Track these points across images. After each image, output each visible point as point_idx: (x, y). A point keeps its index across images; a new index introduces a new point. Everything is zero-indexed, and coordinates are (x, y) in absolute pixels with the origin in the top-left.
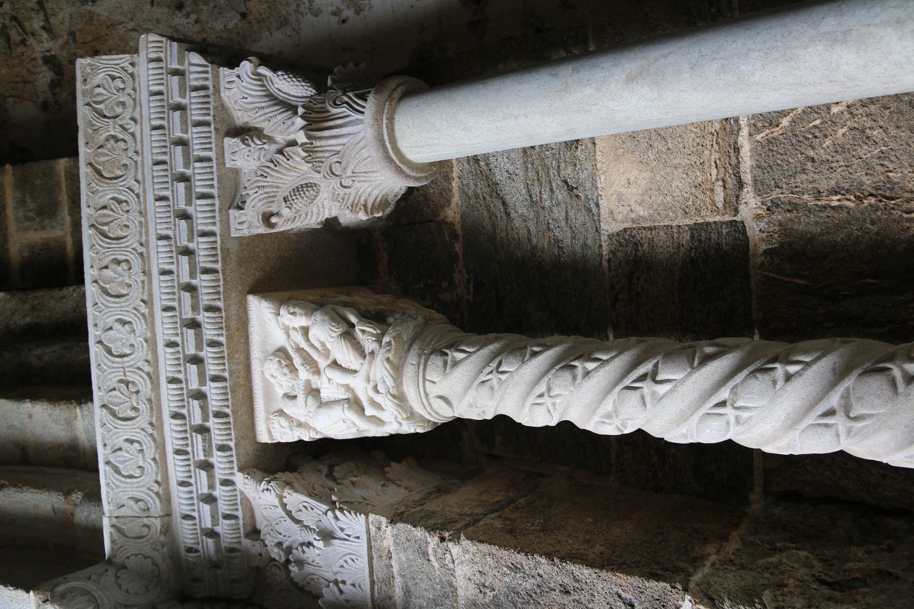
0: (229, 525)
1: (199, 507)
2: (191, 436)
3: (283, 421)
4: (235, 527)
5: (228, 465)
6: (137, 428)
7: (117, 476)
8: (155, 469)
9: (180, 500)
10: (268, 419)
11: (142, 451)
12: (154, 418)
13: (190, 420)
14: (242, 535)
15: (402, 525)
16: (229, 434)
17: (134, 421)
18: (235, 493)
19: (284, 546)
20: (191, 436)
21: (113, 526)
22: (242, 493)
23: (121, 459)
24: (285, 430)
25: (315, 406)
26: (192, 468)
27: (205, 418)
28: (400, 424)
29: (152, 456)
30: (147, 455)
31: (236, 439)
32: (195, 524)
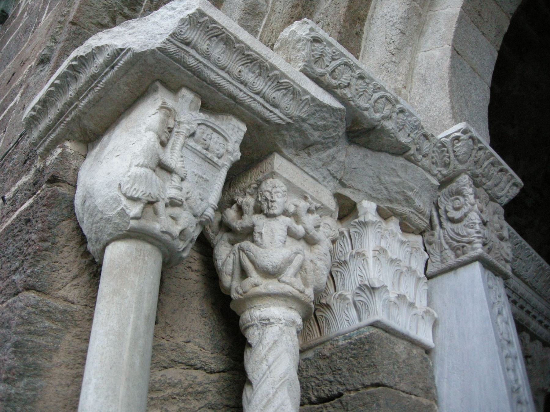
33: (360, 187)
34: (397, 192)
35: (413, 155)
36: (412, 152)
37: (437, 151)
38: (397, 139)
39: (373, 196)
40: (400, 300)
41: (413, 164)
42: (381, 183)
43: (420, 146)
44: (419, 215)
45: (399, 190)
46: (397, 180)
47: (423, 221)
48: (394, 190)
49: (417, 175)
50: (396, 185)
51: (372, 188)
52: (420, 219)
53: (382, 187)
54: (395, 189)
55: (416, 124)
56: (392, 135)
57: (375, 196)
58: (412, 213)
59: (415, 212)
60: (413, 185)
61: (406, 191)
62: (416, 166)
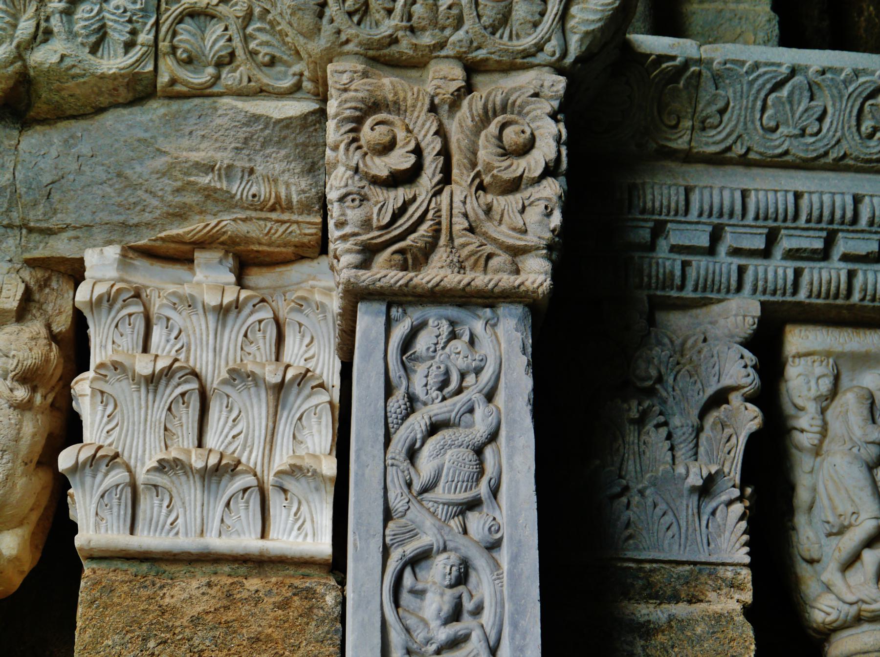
0: (672, 273)
1: (704, 223)
2: (822, 230)
3: (825, 385)
4: (668, 283)
5: (770, 286)
6: (843, 134)
7: (769, 86)
8: (770, 152)
9: (718, 188)
10: (828, 354)
11: (803, 133)
12: (851, 162)
13: (848, 231)
14: (652, 292)
15: (751, 634)
16: (819, 296)
17: (854, 129)
18: (724, 291)
19: (658, 386)
20: (822, 230)
21: (687, 63)
22: (720, 301)
23: (796, 98)
24: (813, 383)
25: (869, 460)
26: (770, 223)
27: (845, 258)
28: (851, 604)
29: (793, 151)
30: (795, 143)
31: (809, 304)
32: (676, 214)
33: (87, 218)
34: (178, 190)
35: (173, 82)
36: (164, 78)
37: (259, 30)
38: (93, 74)
39: (131, 222)
40: (171, 473)
41: (197, 101)
42: (135, 187)
43: (185, 51)
44: (274, 216)
45: (179, 184)
46: (160, 162)
47: (297, 222)
48: (169, 189)
49: (219, 121)
50: (164, 174)
51: (119, 205)
52: (283, 222)
53: (140, 193)
54: (168, 184)
55: (138, 6)
56: (73, 71)
57: (136, 220)
58: (244, 220)
59: (254, 214)
60: (209, 154)
61: (192, 179)
62: (208, 102)
